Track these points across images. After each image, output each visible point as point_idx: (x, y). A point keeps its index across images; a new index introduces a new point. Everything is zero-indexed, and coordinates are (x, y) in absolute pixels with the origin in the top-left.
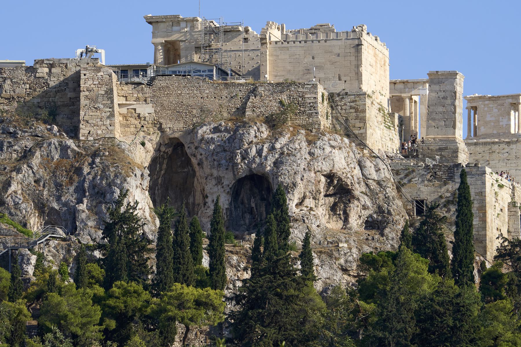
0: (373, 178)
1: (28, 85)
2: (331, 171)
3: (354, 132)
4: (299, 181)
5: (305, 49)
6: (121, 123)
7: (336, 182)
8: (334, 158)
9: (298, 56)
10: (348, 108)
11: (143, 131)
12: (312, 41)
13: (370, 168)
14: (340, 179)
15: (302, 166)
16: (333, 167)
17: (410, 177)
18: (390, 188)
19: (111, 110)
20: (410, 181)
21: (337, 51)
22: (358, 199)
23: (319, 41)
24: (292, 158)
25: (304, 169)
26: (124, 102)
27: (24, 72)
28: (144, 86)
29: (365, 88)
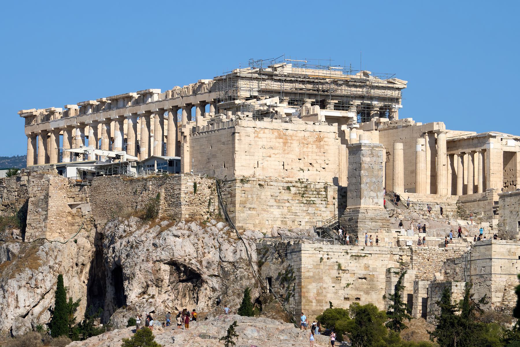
0: (226, 260)
1: (16, 193)
2: (171, 259)
3: (229, 216)
4: (137, 271)
5: (207, 139)
6: (69, 222)
7: (183, 269)
8: (174, 248)
9: (203, 147)
10: (227, 193)
11: (84, 229)
12: (211, 131)
13: (225, 251)
14: (185, 266)
15: (142, 258)
16: (173, 255)
17: (266, 256)
18: (243, 268)
19: (46, 213)
20: (266, 260)
21: (223, 140)
22: (207, 282)
23: (214, 131)
24: (136, 250)
25: (143, 260)
26: (73, 203)
27: (15, 181)
28: (86, 187)
29: (239, 172)
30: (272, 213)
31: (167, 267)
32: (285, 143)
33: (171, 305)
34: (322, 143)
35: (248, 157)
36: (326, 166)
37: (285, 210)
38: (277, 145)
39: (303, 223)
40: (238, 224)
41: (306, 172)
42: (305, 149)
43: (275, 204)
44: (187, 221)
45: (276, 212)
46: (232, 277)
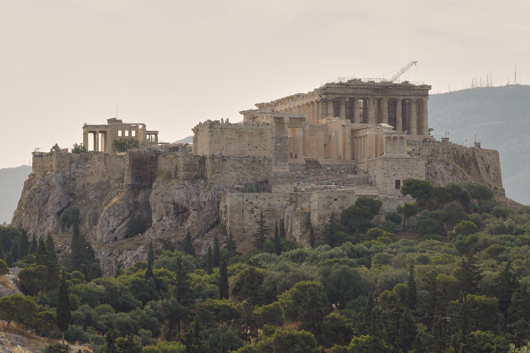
30: (231, 175)
31: (171, 206)
32: (240, 136)
33: (174, 226)
34: (263, 135)
35: (217, 145)
36: (265, 148)
37: (239, 173)
38: (235, 137)
39: (249, 180)
40: (209, 181)
41: (253, 152)
42: (252, 139)
43: (233, 169)
44: (185, 180)
45: (234, 174)
46: (203, 210)
